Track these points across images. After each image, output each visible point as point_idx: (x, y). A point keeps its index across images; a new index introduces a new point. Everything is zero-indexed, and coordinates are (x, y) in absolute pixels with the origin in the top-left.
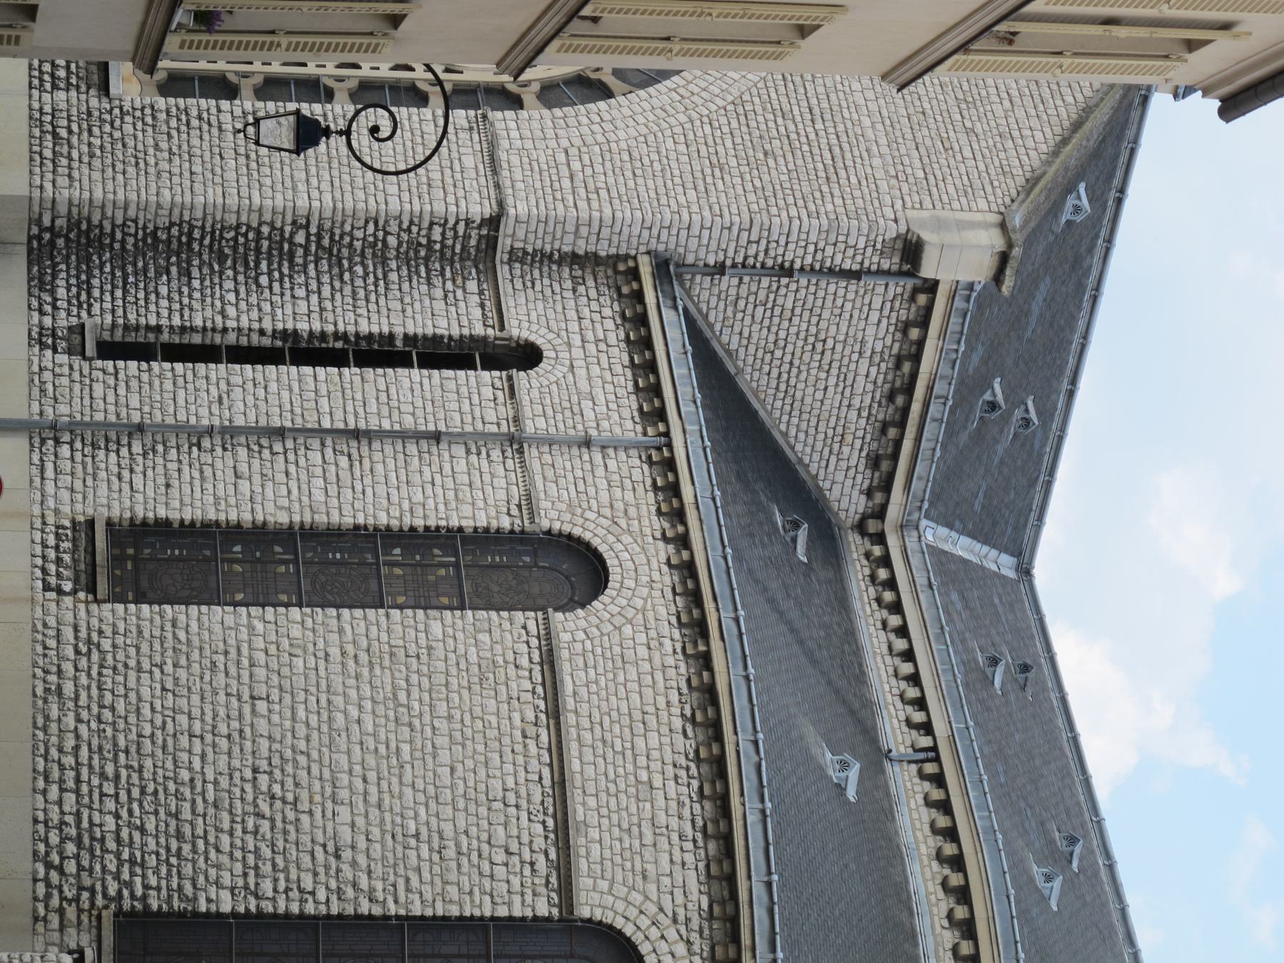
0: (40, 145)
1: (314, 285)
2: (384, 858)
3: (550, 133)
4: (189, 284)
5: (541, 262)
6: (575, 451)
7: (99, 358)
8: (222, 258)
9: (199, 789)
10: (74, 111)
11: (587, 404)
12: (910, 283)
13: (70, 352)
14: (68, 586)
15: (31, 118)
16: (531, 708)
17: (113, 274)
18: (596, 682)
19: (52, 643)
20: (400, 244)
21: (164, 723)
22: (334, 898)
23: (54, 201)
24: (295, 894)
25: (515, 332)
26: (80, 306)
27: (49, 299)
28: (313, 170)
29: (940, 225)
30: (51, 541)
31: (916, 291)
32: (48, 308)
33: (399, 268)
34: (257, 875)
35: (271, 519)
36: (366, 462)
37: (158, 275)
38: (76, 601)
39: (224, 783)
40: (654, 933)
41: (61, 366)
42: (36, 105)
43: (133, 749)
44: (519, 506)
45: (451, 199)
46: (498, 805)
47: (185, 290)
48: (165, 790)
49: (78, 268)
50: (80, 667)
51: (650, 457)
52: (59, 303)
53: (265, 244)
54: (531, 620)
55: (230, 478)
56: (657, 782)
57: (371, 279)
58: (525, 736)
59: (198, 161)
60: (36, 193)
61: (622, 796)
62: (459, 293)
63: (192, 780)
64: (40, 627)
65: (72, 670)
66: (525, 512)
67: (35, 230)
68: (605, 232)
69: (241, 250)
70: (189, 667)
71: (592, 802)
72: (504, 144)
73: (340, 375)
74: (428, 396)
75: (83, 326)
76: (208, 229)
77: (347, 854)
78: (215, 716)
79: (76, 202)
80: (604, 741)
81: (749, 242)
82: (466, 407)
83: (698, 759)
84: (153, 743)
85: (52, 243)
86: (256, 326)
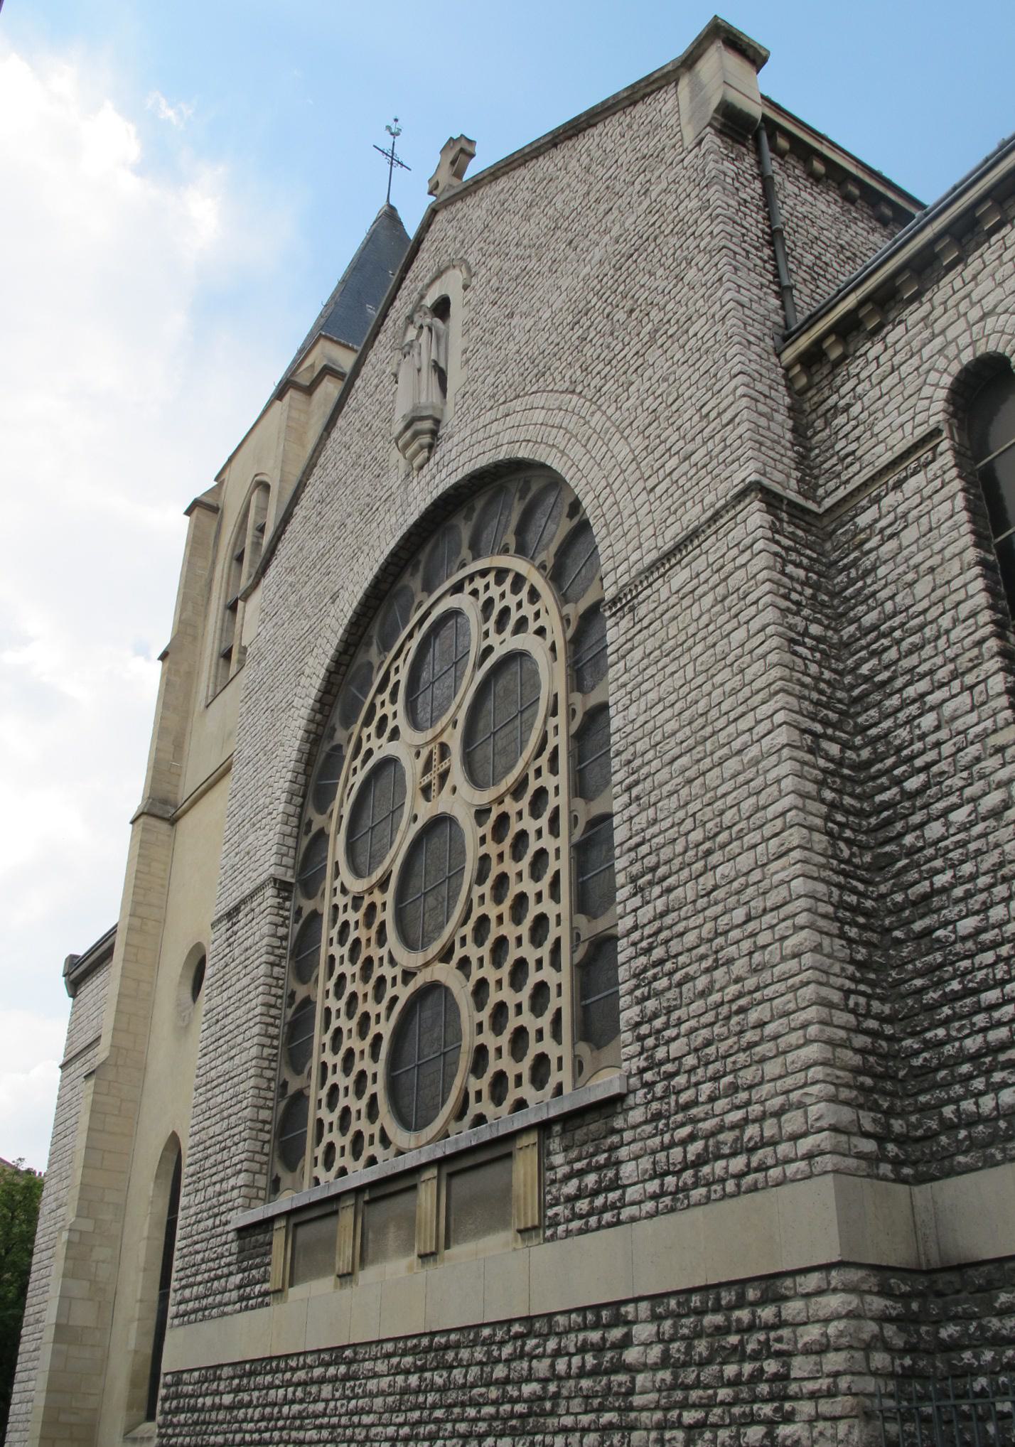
0: (723, 1181)
4: (945, 890)
5: (812, 469)
15: (672, 1210)
17: (946, 1022)
23: (834, 1129)
31: (774, 149)
42: (649, 1206)
47: (958, 892)
49: (946, 1085)
59: (723, 921)
60: (827, 1162)
68: (759, 386)
69: (862, 838)
76: (841, 879)
79: (832, 1089)
81: (748, 258)
85: (901, 1140)
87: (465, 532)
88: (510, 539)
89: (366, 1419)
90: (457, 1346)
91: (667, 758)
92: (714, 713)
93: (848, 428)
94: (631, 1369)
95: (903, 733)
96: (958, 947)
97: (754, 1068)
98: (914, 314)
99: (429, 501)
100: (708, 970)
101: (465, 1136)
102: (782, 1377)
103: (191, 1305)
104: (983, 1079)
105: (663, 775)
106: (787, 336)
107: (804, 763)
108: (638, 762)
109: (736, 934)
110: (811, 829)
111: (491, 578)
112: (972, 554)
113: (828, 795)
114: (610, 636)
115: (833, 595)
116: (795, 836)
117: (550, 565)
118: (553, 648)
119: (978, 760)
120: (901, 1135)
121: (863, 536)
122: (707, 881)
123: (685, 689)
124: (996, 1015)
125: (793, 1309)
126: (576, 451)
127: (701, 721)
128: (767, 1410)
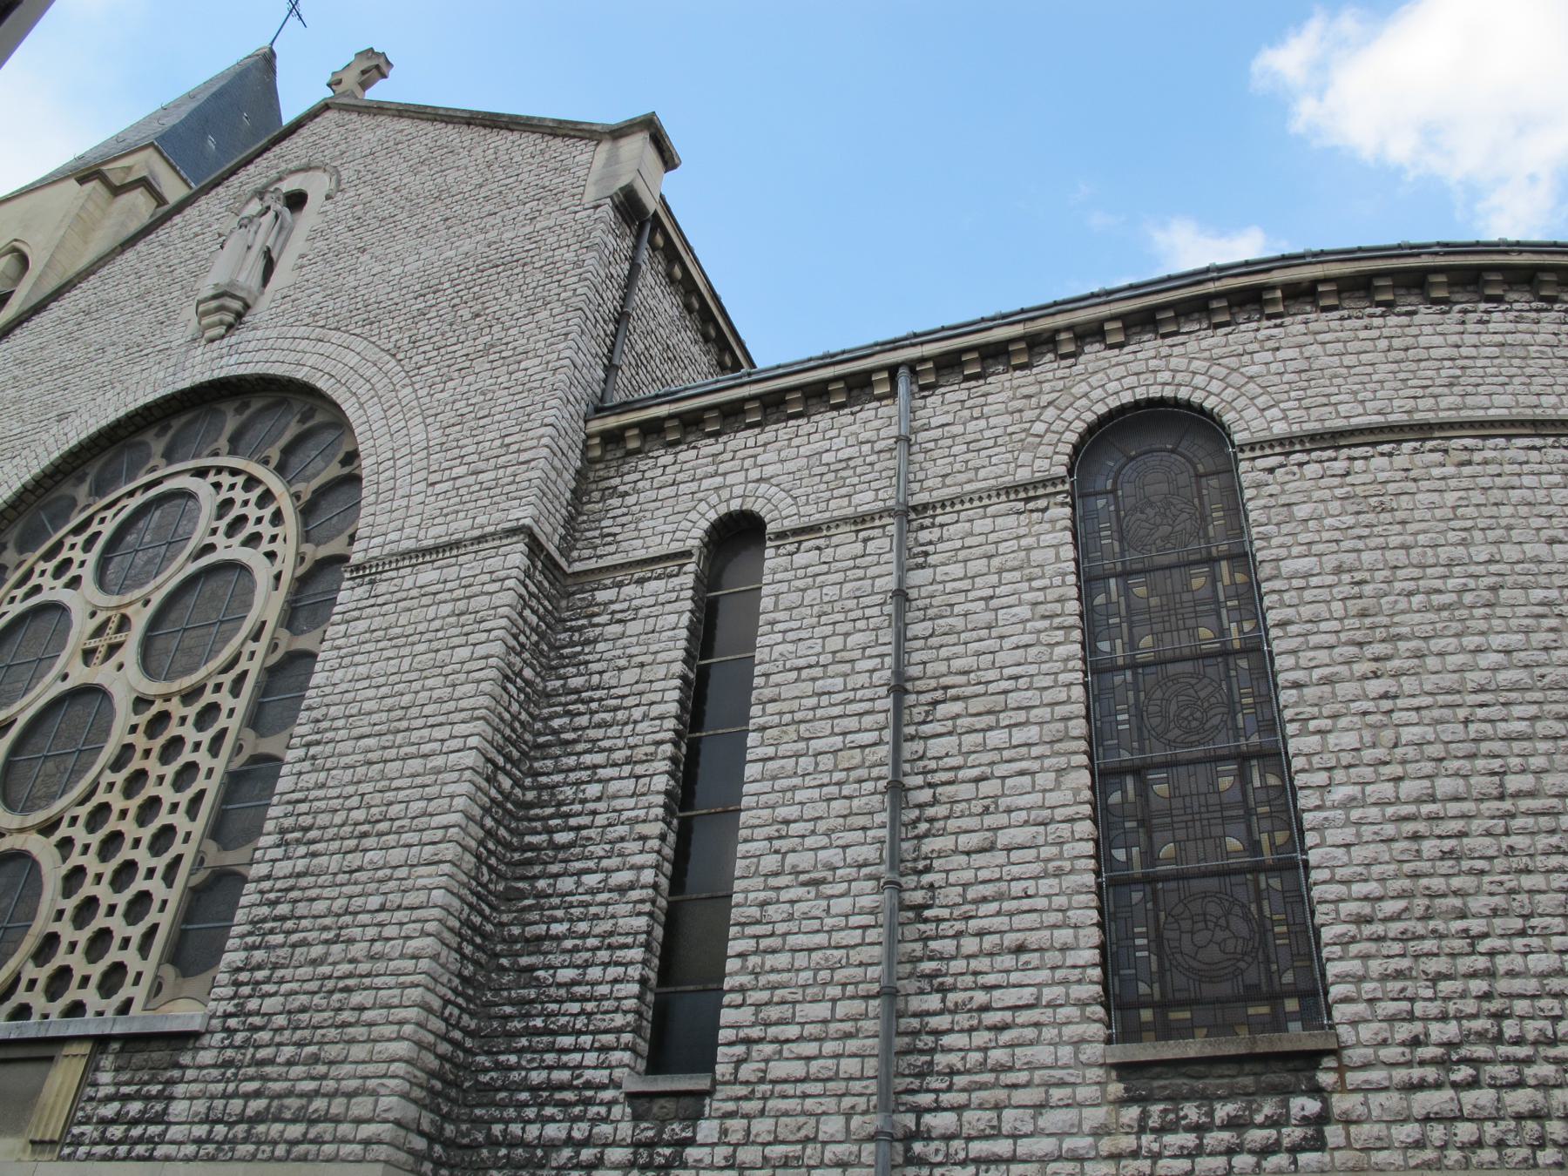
0: (275, 1143)
4: (558, 938)
7: (713, 1071)
8: (511, 896)
13: (699, 1116)
14: (1312, 1106)
15: (212, 1158)
17: (520, 1051)
23: (398, 1123)
25: (697, 543)
26: (588, 1102)
27: (567, 1153)
31: (651, 242)
32: (587, 1154)
41: (724, 1132)
42: (190, 1149)
44: (1027, 500)
47: (568, 944)
49: (502, 1105)
50: (1514, 1077)
51: (923, 388)
52: (576, 1134)
54: (1249, 472)
55: (1000, 857)
58: (1469, 463)
59: (359, 901)
60: (382, 1151)
65: (1521, 1092)
66: (1041, 492)
68: (562, 443)
69: (503, 868)
75: (632, 1097)
76: (474, 900)
79: (407, 1085)
85: (448, 1144)
87: (231, 424)
91: (355, 733)
92: (414, 711)
93: (619, 512)
95: (569, 792)
96: (552, 990)
97: (340, 1046)
98: (709, 447)
99: (207, 377)
100: (326, 942)
104: (535, 1110)
105: (347, 746)
106: (600, 409)
107: (479, 788)
109: (364, 918)
110: (465, 848)
111: (240, 480)
112: (678, 668)
113: (489, 822)
114: (342, 596)
115: (552, 647)
116: (450, 851)
117: (306, 497)
118: (278, 577)
119: (622, 839)
120: (449, 1139)
121: (596, 609)
122: (354, 860)
123: (396, 678)
124: (565, 1058)
126: (375, 412)
127: (400, 713)
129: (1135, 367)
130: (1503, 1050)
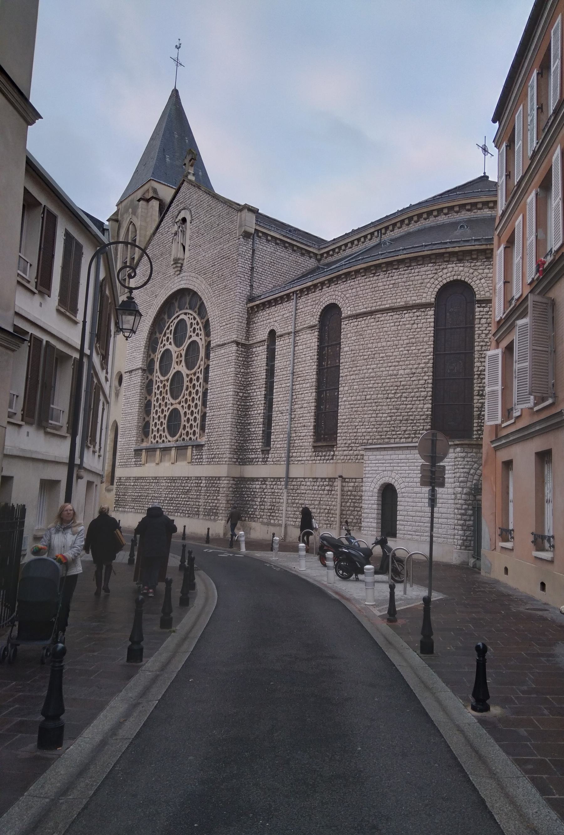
1: (253, 391)
2: (415, 360)
3: (216, 331)
4: (252, 423)
5: (249, 333)
6: (297, 317)
8: (246, 415)
9: (393, 414)
10: (208, 453)
11: (285, 316)
12: (256, 237)
14: (332, 453)
16: (370, 320)
17: (249, 443)
18: (363, 302)
19: (349, 457)
20: (243, 369)
21: (373, 425)
22: (427, 374)
24: (426, 386)
25: (266, 337)
28: (224, 391)
29: (241, 226)
30: (319, 458)
31: (258, 236)
32: (257, 460)
33: (250, 369)
34: (420, 397)
35: (314, 398)
36: (299, 373)
37: (250, 431)
38: (336, 451)
39: (391, 407)
40: (440, 279)
43: (381, 434)
44: (312, 330)
45: (231, 355)
46: (399, 328)
47: (253, 424)
48: (393, 424)
49: (247, 452)
51: (299, 297)
53: (242, 403)
56: (393, 282)
57: (252, 376)
58: (378, 321)
61: (397, 292)
62: (256, 353)
63: (390, 417)
64: (344, 461)
67: (237, 463)
68: (241, 315)
69: (244, 410)
70: (356, 418)
71: (399, 300)
72: (219, 343)
73: (276, 382)
74: (282, 358)
75: (262, 450)
77: (414, 371)
78: (370, 410)
80: (380, 298)
81: (244, 277)
82: (285, 348)
83: (386, 271)
84: (379, 428)
85: (241, 459)
86: (263, 405)
88: (196, 309)
89: (161, 490)
90: (177, 480)
94: (202, 487)
101: (180, 443)
102: (219, 491)
103: (123, 463)
105: (216, 390)
107: (234, 398)
108: (212, 385)
109: (222, 424)
111: (192, 317)
115: (248, 362)
122: (219, 413)
125: (221, 481)
128: (216, 494)
129: (330, 294)
130: (356, 445)
